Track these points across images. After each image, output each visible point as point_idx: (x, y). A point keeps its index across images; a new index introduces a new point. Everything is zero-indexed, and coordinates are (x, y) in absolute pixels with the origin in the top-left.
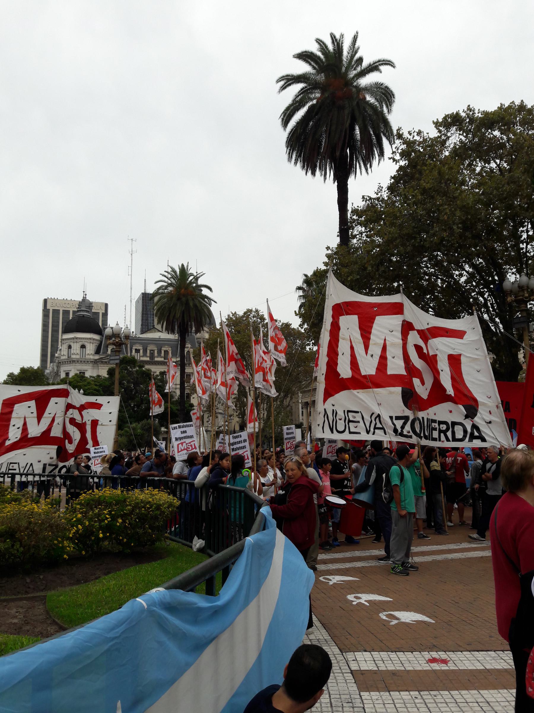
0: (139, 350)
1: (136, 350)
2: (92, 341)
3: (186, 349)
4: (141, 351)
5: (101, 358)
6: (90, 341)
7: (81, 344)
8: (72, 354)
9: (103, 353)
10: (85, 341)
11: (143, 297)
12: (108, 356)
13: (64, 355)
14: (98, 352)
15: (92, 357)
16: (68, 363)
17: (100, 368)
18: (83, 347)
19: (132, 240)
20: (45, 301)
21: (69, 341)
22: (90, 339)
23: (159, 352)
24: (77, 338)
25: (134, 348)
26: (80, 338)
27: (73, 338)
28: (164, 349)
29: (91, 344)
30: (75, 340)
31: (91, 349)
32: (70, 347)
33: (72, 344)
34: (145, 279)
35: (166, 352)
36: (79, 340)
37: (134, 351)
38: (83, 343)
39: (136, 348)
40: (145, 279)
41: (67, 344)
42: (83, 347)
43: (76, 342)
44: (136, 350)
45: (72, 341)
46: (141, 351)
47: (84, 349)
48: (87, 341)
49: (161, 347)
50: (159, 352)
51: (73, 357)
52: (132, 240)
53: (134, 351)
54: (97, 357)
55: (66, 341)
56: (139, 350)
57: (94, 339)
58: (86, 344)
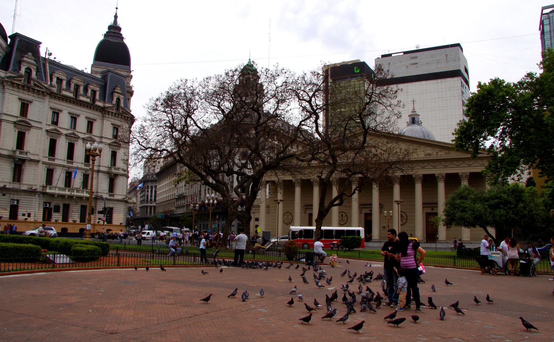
1: (58, 78)
3: (116, 94)
4: (64, 83)
9: (14, 70)
17: (7, 91)
23: (86, 90)
25: (56, 75)
28: (91, 87)
35: (94, 92)
37: (55, 80)
39: (58, 76)
44: (58, 78)
46: (64, 83)
49: (88, 84)
50: (86, 90)
53: (55, 80)
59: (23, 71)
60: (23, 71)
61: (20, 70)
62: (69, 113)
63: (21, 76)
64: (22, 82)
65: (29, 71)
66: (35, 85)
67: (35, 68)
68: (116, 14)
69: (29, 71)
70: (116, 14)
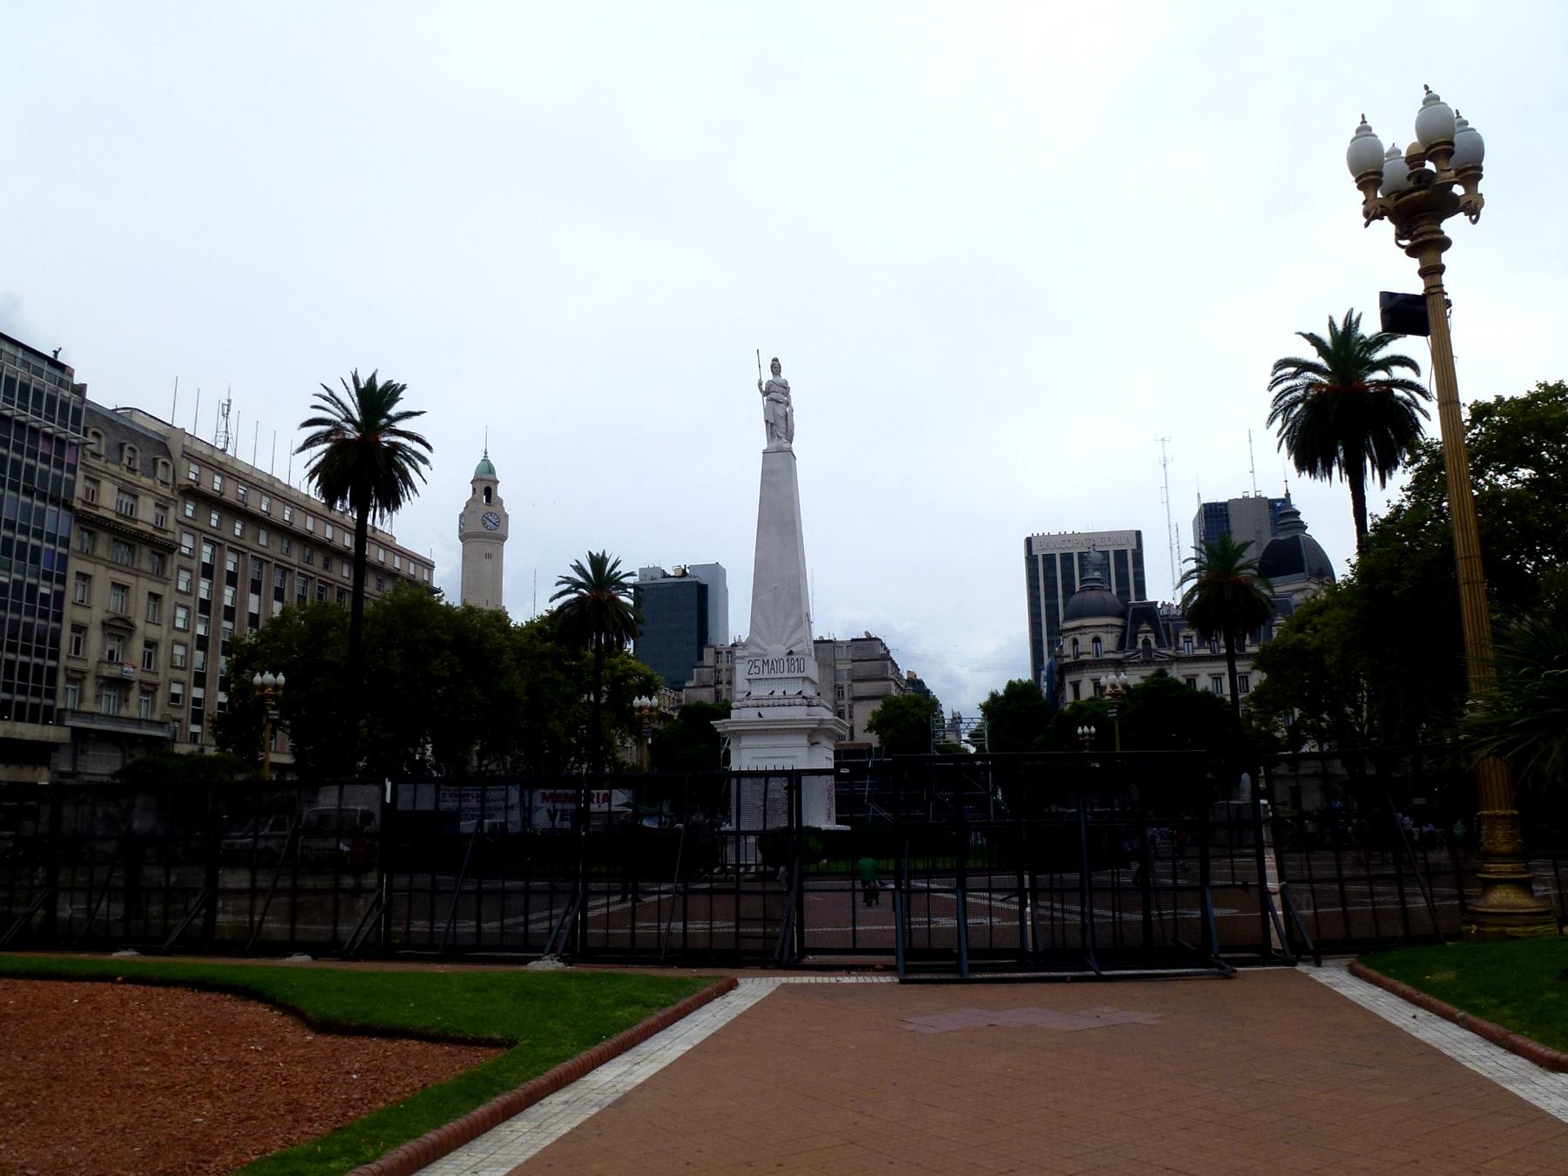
0: (1191, 637)
2: (1109, 629)
5: (1128, 657)
6: (1107, 629)
8: (1083, 653)
10: (1099, 629)
11: (1205, 512)
12: (1138, 652)
13: (1068, 656)
14: (1121, 646)
15: (1111, 656)
16: (1075, 670)
18: (1097, 640)
19: (1163, 440)
20: (1029, 541)
21: (1073, 633)
22: (1107, 626)
24: (1085, 627)
25: (1182, 634)
26: (1089, 627)
29: (1110, 635)
31: (1109, 641)
32: (1075, 642)
33: (1078, 637)
34: (1199, 494)
36: (1089, 630)
38: (1096, 633)
39: (1184, 634)
40: (1199, 494)
41: (1070, 637)
42: (1097, 640)
43: (1085, 634)
44: (1185, 637)
45: (1078, 632)
47: (1099, 644)
48: (1102, 629)
51: (1083, 657)
52: (1163, 440)
53: (1181, 640)
54: (1120, 656)
55: (1070, 633)
56: (1191, 637)
57: (1112, 625)
58: (1101, 635)
59: (1140, 646)
60: (1140, 646)
61: (1137, 644)
62: (1210, 675)
63: (1138, 652)
64: (1141, 657)
65: (1146, 642)
66: (1156, 656)
67: (1153, 635)
68: (1287, 490)
69: (1146, 642)
70: (1287, 490)
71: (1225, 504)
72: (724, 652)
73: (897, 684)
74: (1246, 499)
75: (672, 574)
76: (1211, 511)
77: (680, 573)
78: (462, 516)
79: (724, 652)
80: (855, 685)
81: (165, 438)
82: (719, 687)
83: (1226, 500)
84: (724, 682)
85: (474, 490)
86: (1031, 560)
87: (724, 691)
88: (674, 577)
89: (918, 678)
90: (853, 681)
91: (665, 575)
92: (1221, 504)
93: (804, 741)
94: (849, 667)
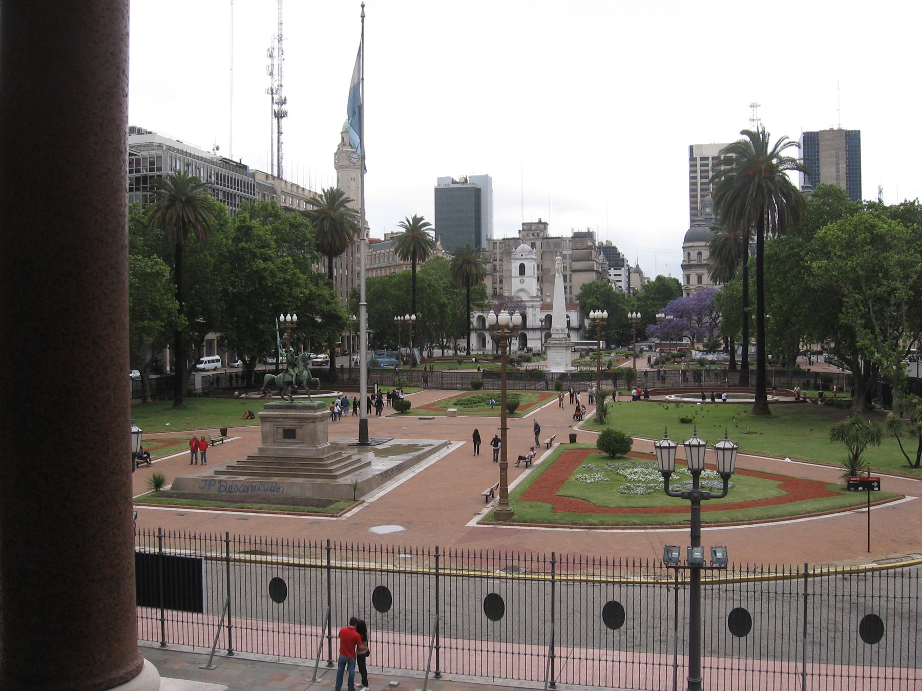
7: (697, 251)
11: (804, 138)
18: (700, 254)
20: (691, 148)
24: (694, 247)
26: (697, 246)
27: (691, 247)
30: (693, 248)
33: (690, 251)
42: (700, 254)
51: (692, 263)
71: (817, 133)
72: (498, 243)
73: (597, 262)
74: (832, 130)
75: (458, 180)
76: (808, 138)
77: (463, 181)
78: (336, 154)
79: (498, 243)
80: (574, 263)
81: (272, 185)
82: (495, 263)
83: (818, 130)
84: (498, 260)
85: (343, 138)
86: (692, 159)
87: (498, 265)
88: (459, 183)
89: (613, 245)
90: (572, 261)
91: (454, 182)
92: (814, 133)
93: (565, 348)
94: (570, 252)
